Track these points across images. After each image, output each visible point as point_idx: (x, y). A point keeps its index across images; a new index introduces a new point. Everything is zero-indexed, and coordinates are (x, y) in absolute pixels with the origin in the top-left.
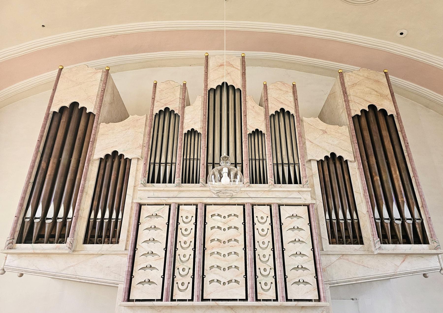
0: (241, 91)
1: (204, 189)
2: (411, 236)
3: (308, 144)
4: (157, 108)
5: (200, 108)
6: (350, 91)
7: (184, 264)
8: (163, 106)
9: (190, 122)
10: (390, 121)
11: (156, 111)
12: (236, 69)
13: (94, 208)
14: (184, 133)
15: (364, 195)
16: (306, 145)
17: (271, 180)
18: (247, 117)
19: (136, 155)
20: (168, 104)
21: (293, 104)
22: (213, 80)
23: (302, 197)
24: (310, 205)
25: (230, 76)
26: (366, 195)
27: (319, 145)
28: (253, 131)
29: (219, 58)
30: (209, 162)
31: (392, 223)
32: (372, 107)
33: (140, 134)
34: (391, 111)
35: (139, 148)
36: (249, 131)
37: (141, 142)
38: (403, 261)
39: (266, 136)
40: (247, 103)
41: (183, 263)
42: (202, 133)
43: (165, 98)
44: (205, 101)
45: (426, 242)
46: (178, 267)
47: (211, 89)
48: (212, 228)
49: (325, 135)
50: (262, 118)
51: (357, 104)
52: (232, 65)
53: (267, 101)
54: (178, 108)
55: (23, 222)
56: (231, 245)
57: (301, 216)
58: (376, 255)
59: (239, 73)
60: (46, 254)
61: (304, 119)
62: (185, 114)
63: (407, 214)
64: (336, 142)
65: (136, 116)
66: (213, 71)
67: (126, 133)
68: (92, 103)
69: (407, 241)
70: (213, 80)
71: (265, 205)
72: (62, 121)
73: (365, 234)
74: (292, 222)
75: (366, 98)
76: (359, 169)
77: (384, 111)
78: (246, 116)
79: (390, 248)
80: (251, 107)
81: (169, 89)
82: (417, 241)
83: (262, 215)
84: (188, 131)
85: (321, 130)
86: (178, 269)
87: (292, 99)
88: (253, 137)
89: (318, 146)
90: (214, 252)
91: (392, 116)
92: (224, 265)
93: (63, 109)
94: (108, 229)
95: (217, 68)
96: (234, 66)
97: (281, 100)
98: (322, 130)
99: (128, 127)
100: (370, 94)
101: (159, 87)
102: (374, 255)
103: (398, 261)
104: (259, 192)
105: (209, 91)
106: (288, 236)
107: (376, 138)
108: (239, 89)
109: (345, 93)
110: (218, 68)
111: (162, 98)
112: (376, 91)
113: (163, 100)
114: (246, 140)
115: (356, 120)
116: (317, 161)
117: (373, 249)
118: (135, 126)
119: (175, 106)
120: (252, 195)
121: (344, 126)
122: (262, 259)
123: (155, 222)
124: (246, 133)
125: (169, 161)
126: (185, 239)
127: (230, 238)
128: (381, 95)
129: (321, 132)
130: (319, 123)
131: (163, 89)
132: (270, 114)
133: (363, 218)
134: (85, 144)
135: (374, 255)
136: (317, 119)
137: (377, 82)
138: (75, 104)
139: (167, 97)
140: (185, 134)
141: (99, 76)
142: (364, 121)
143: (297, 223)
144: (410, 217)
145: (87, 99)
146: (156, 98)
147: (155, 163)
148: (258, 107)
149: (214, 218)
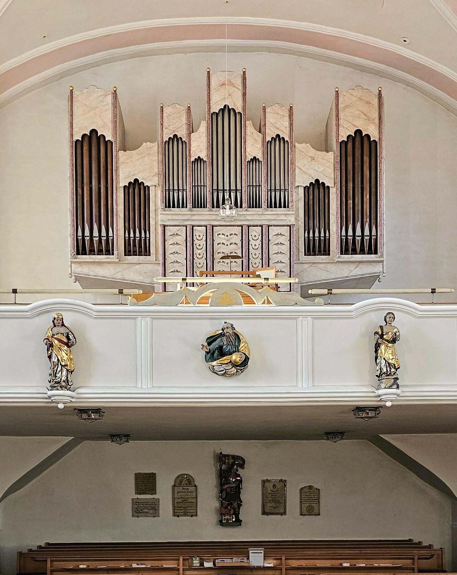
0: (241, 114)
1: (211, 213)
3: (297, 171)
4: (167, 135)
5: (205, 135)
6: (341, 115)
8: (171, 134)
9: (196, 150)
10: (373, 145)
11: (166, 139)
12: (237, 89)
14: (192, 161)
16: (295, 172)
18: (247, 143)
19: (154, 183)
20: (176, 131)
21: (288, 129)
25: (231, 97)
27: (306, 171)
28: (251, 159)
29: (220, 75)
30: (214, 188)
32: (358, 132)
33: (154, 162)
34: (374, 136)
39: (262, 162)
40: (246, 128)
42: (207, 161)
43: (173, 124)
44: (209, 127)
47: (214, 113)
49: (313, 162)
50: (259, 145)
51: (345, 129)
53: (265, 126)
54: (185, 136)
61: (297, 145)
62: (191, 141)
65: (148, 143)
66: (216, 91)
68: (109, 130)
70: (215, 103)
72: (84, 148)
75: (354, 123)
77: (368, 136)
78: (245, 142)
80: (250, 133)
81: (175, 114)
84: (196, 159)
85: (310, 157)
89: (306, 173)
91: (374, 141)
93: (84, 136)
95: (219, 87)
96: (236, 86)
97: (277, 126)
98: (311, 157)
99: (144, 155)
100: (359, 117)
101: (166, 112)
105: (212, 114)
108: (239, 113)
109: (337, 116)
110: (220, 88)
111: (170, 124)
112: (365, 115)
113: (171, 126)
114: (245, 167)
115: (343, 146)
118: (150, 155)
119: (182, 133)
121: (330, 152)
124: (245, 161)
125: (181, 188)
129: (310, 159)
130: (308, 149)
131: (170, 114)
132: (267, 141)
134: (109, 172)
136: (308, 146)
138: (94, 131)
140: (193, 161)
141: (110, 99)
145: (103, 126)
147: (169, 190)
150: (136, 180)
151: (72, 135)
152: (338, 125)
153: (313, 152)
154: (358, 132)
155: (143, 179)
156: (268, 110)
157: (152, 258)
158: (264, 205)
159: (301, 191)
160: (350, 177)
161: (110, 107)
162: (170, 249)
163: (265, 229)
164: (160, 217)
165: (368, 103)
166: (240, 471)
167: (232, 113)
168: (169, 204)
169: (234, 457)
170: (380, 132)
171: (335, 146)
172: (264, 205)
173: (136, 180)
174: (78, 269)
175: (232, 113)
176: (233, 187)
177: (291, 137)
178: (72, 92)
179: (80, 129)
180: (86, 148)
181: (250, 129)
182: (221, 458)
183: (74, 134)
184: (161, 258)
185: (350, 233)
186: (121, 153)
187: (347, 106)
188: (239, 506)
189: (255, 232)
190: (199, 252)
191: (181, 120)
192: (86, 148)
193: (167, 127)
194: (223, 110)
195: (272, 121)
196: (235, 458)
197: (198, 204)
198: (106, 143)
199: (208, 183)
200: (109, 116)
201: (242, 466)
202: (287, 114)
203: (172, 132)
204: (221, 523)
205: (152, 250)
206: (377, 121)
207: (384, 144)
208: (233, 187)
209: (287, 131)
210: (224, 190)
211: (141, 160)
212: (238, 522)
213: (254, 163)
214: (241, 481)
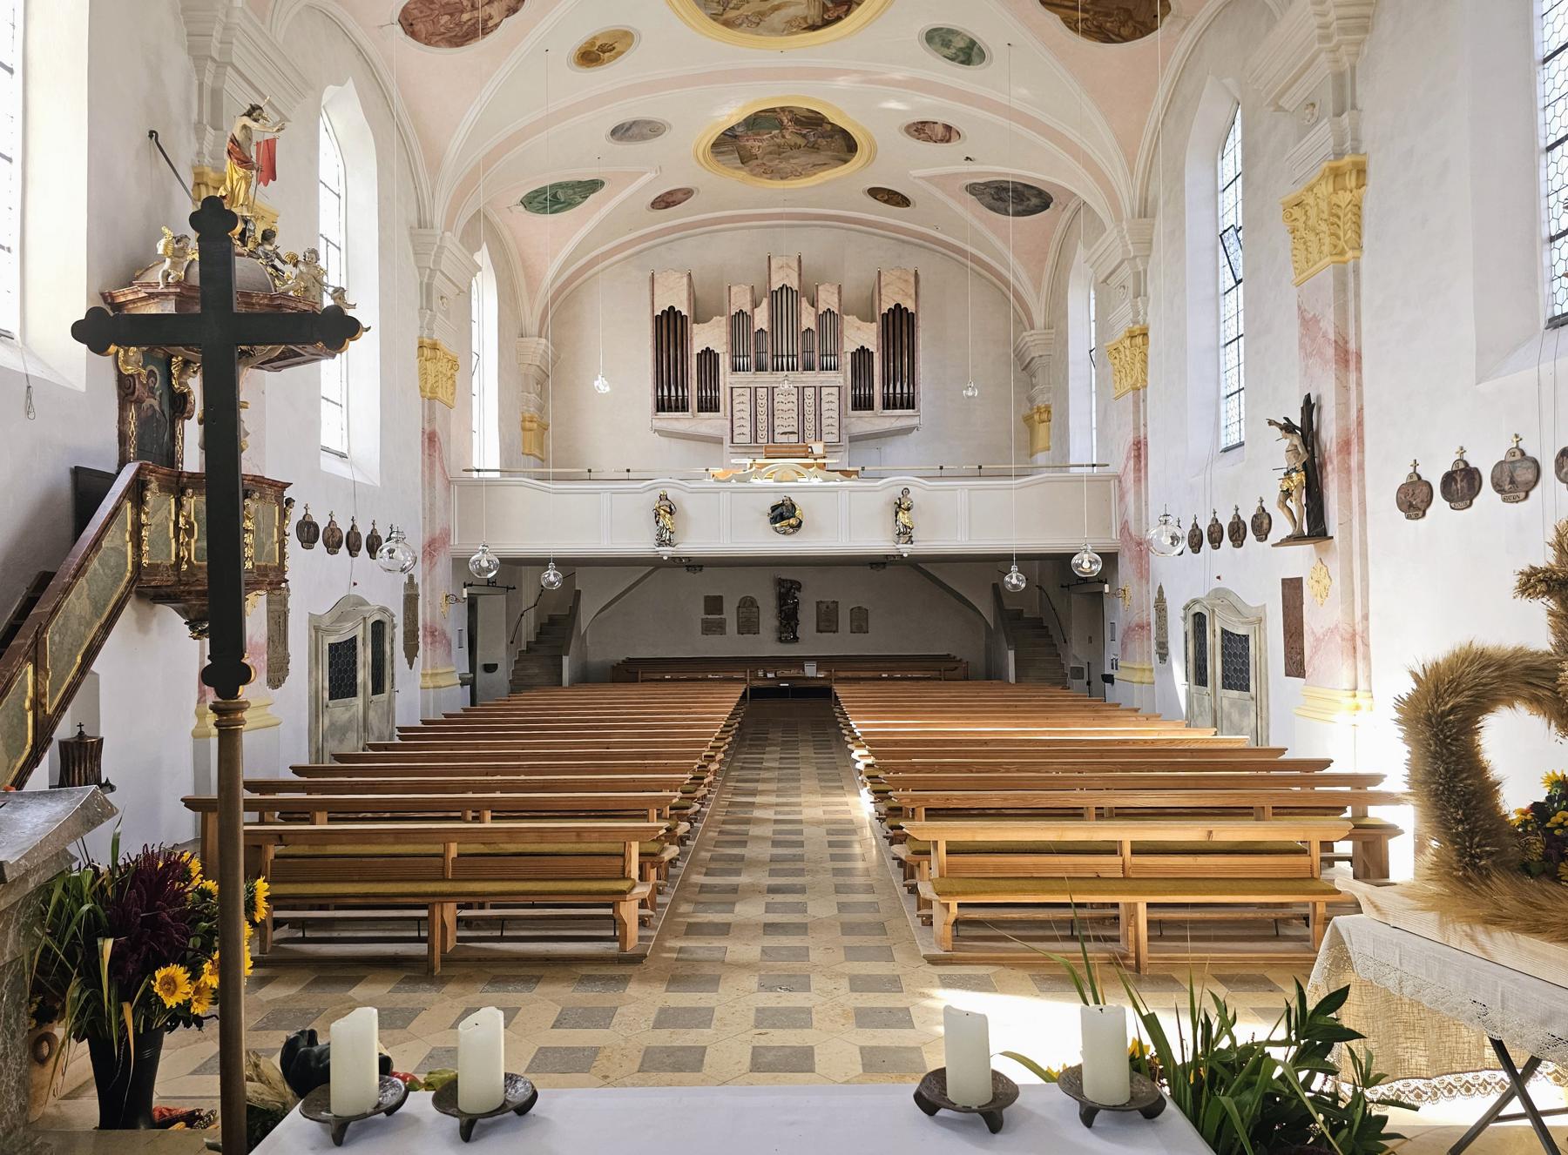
6: (883, 291)
13: (699, 389)
31: (894, 397)
32: (898, 305)
34: (911, 309)
45: (913, 408)
50: (813, 318)
59: (796, 275)
61: (845, 317)
63: (905, 390)
64: (866, 337)
69: (902, 407)
77: (906, 309)
79: (888, 412)
82: (908, 408)
87: (837, 300)
92: (785, 424)
94: (711, 403)
103: (893, 420)
106: (825, 406)
107: (898, 331)
119: (747, 308)
123: (741, 399)
128: (906, 294)
137: (906, 281)
138: (672, 308)
141: (685, 280)
142: (891, 317)
143: (831, 398)
148: (810, 308)
150: (708, 348)
152: (880, 300)
153: (858, 322)
154: (898, 305)
156: (820, 288)
157: (721, 414)
158: (817, 369)
159: (849, 356)
160: (891, 344)
161: (685, 287)
162: (737, 407)
163: (818, 391)
164: (728, 380)
165: (906, 281)
166: (797, 594)
167: (789, 291)
168: (736, 368)
169: (791, 581)
170: (917, 306)
171: (878, 318)
172: (817, 369)
173: (708, 348)
174: (658, 424)
175: (789, 291)
176: (790, 353)
177: (839, 310)
180: (664, 321)
181: (805, 303)
182: (780, 582)
184: (729, 414)
185: (891, 391)
186: (695, 325)
187: (888, 284)
188: (797, 624)
189: (809, 392)
190: (762, 410)
192: (664, 321)
194: (782, 289)
195: (824, 297)
196: (793, 582)
197: (760, 368)
198: (682, 317)
199: (769, 351)
200: (684, 295)
201: (799, 589)
202: (836, 292)
204: (780, 640)
205: (722, 408)
206: (914, 296)
207: (920, 315)
208: (790, 353)
209: (837, 305)
210: (782, 356)
212: (796, 639)
214: (798, 603)
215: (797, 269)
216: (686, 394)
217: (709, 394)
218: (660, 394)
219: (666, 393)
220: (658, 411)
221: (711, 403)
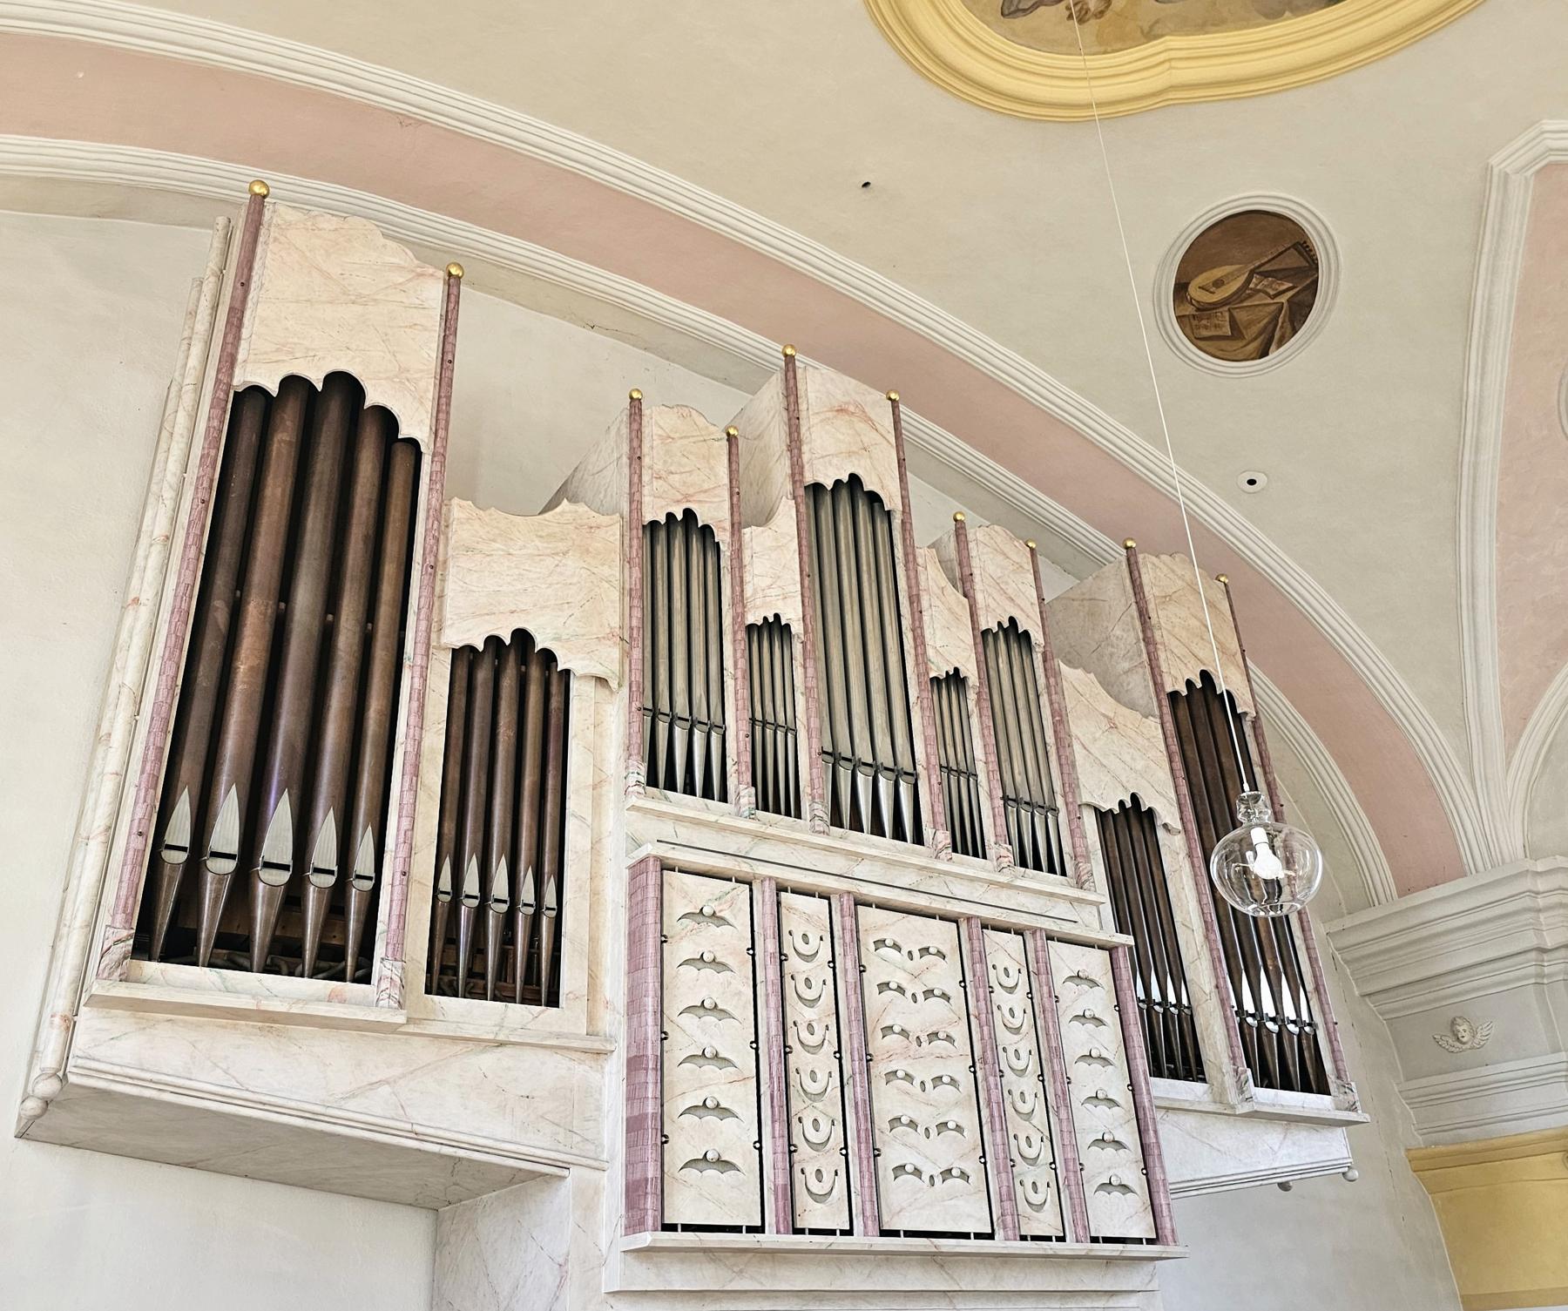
2: (1295, 1070)
7: (815, 1104)
12: (885, 442)
15: (1207, 937)
17: (1008, 850)
20: (695, 498)
22: (822, 457)
23: (1080, 922)
24: (1117, 948)
25: (871, 458)
26: (1212, 937)
29: (832, 380)
33: (607, 585)
35: (608, 642)
36: (932, 666)
37: (615, 621)
38: (1284, 1138)
41: (814, 1101)
46: (799, 1115)
48: (884, 986)
52: (870, 419)
55: (156, 863)
56: (937, 1052)
57: (1097, 979)
58: (1240, 1115)
60: (270, 1020)
64: (1140, 765)
67: (558, 569)
70: (822, 457)
71: (1007, 931)
73: (1211, 1053)
74: (1080, 995)
76: (1190, 855)
81: (692, 440)
83: (1008, 963)
86: (800, 1120)
88: (944, 692)
89: (1102, 764)
90: (895, 1069)
99: (562, 546)
101: (656, 423)
102: (1235, 1115)
104: (976, 884)
110: (835, 417)
113: (677, 477)
116: (1096, 810)
117: (1232, 1096)
119: (716, 512)
120: (960, 890)
122: (1020, 1105)
123: (709, 940)
126: (809, 1014)
127: (934, 1029)
129: (1105, 725)
133: (1204, 1005)
134: (390, 570)
135: (1235, 1115)
139: (687, 469)
141: (435, 292)
144: (1293, 1017)
145: (397, 376)
146: (646, 461)
149: (883, 951)
151: (229, 361)
155: (558, 639)
178: (262, 205)
179: (277, 350)
183: (240, 357)
191: (712, 469)
193: (663, 474)
195: (991, 569)
203: (680, 497)
211: (550, 562)
213: (944, 692)
215: (893, 441)
216: (363, 861)
217: (500, 887)
218: (180, 830)
219: (226, 832)
220: (142, 948)
221: (478, 949)
